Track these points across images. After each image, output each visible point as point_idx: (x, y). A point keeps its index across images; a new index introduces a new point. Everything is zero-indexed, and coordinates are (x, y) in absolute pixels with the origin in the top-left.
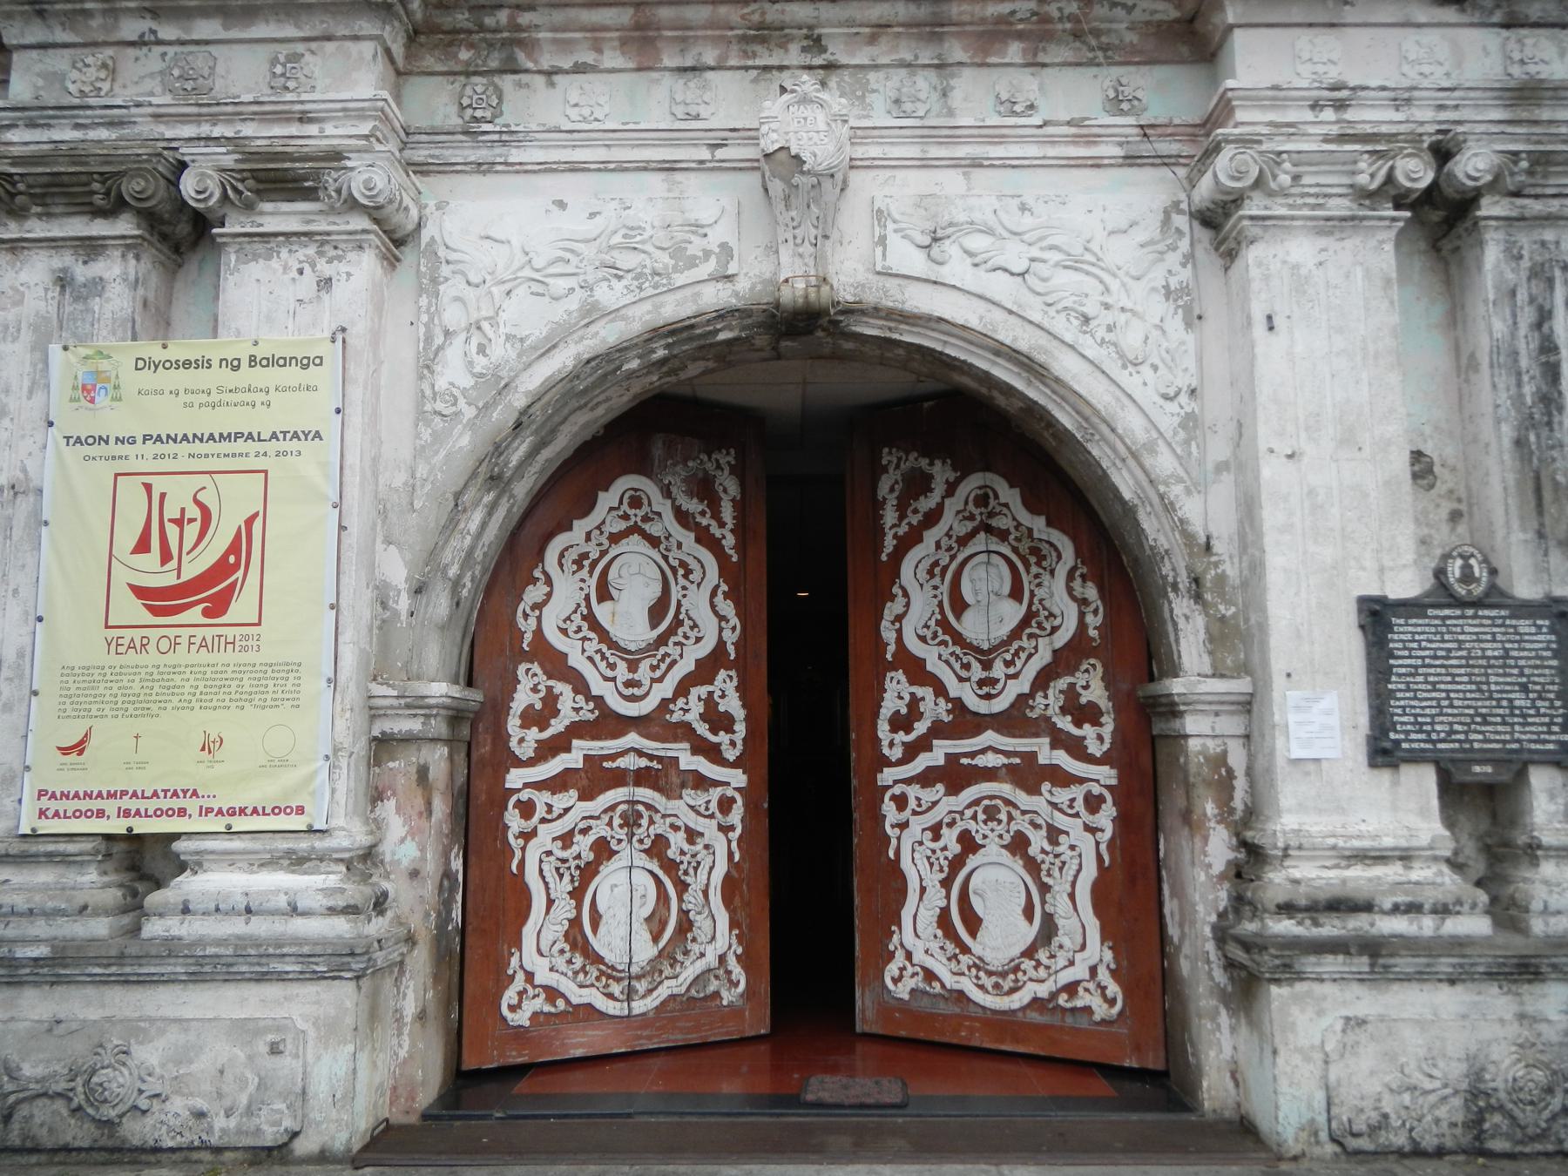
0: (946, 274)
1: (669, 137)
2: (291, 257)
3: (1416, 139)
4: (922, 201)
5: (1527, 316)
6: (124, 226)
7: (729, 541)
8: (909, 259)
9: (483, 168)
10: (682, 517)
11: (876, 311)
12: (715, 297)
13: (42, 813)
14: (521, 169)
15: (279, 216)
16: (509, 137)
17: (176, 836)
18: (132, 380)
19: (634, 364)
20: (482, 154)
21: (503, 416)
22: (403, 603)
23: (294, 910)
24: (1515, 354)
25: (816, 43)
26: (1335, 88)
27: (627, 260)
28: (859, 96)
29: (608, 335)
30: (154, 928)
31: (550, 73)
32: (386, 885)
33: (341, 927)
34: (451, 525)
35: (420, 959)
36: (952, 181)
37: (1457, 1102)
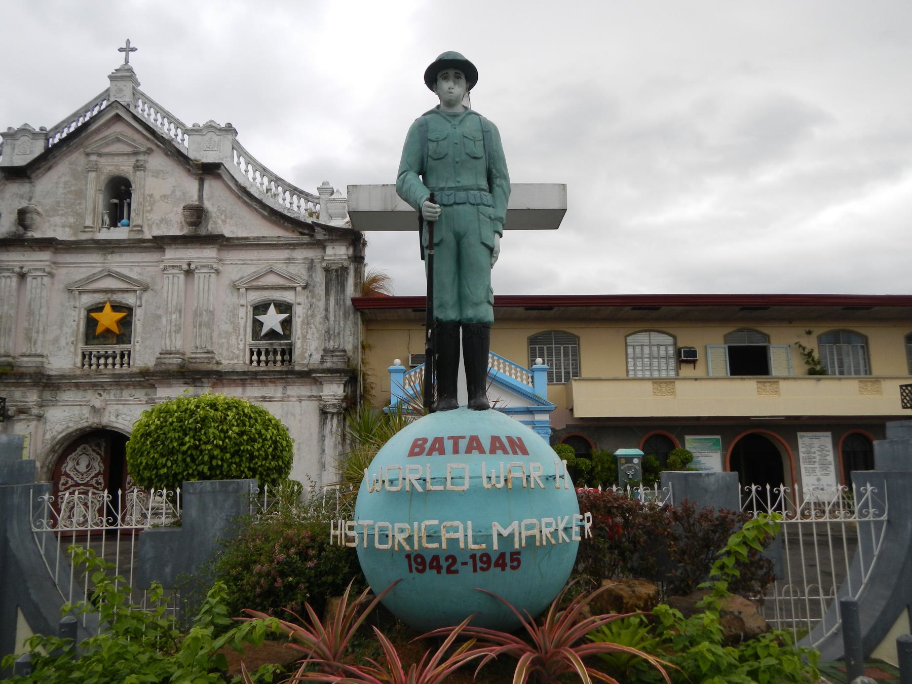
0: (118, 421)
1: (80, 401)
4: (117, 410)
7: (103, 454)
8: (113, 418)
9: (53, 405)
10: (94, 450)
11: (109, 426)
12: (86, 424)
14: (58, 406)
15: (22, 416)
16: (57, 401)
21: (54, 442)
25: (103, 387)
27: (73, 419)
28: (109, 393)
29: (70, 430)
34: (46, 458)
36: (121, 407)
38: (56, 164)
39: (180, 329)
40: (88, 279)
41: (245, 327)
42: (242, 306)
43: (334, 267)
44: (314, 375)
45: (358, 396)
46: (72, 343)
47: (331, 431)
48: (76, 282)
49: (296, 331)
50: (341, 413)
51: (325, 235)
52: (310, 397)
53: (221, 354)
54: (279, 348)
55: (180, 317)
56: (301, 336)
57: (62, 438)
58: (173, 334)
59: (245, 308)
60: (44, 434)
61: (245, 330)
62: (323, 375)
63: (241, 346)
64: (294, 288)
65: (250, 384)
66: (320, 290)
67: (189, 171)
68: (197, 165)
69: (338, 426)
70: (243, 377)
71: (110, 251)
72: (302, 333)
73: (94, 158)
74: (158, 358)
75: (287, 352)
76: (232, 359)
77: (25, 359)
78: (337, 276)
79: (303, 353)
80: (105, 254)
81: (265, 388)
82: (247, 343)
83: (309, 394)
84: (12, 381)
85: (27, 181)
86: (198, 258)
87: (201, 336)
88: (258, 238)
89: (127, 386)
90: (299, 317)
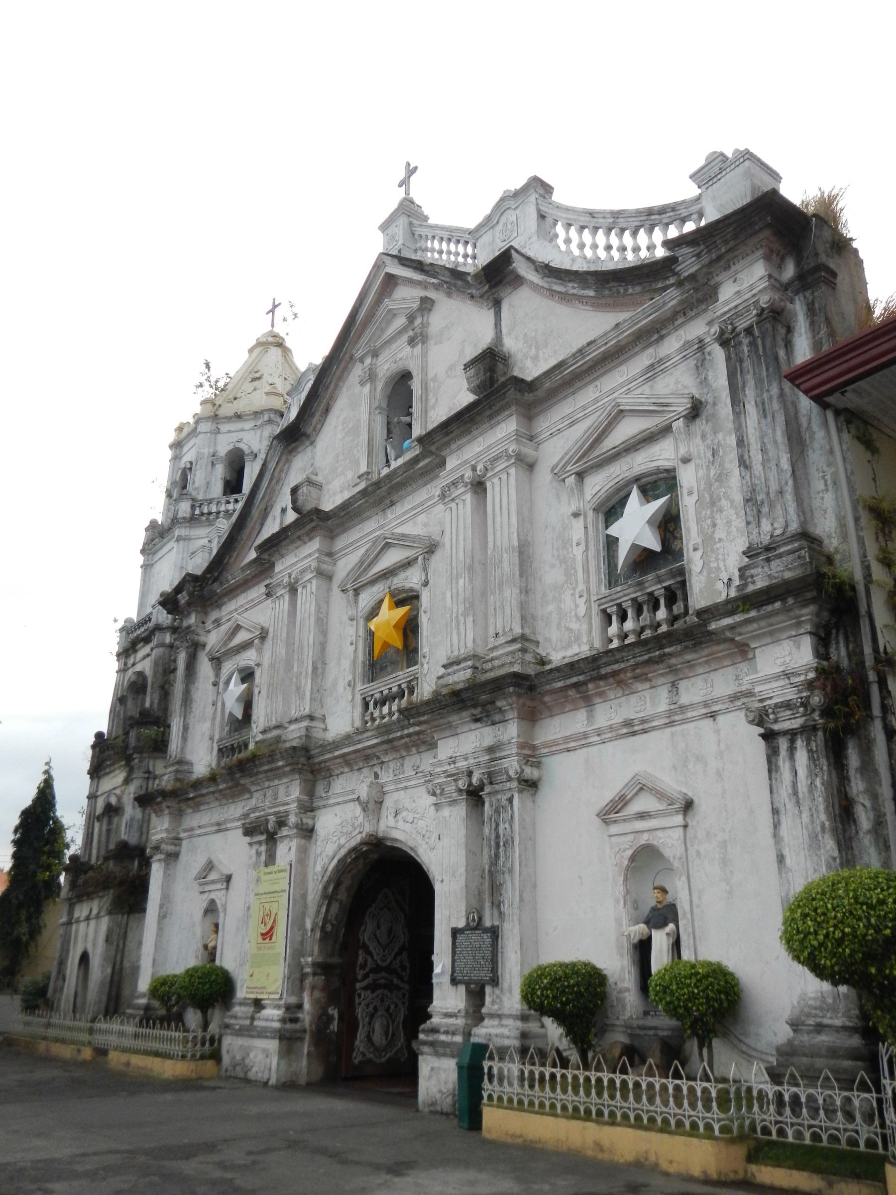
2: (286, 841)
3: (463, 773)
5: (494, 825)
6: (263, 837)
9: (324, 806)
12: (358, 839)
13: (247, 993)
15: (285, 831)
16: (328, 798)
17: (261, 1000)
18: (264, 878)
19: (349, 860)
20: (323, 803)
21: (326, 879)
22: (309, 934)
23: (273, 1020)
24: (490, 840)
25: (378, 758)
26: (451, 758)
29: (343, 852)
30: (256, 1023)
31: (338, 775)
32: (300, 1015)
33: (277, 1025)
34: (318, 912)
35: (307, 1037)
37: (450, 1097)
38: (332, 399)
39: (472, 605)
40: (363, 563)
41: (586, 562)
42: (576, 515)
43: (742, 324)
44: (713, 626)
45: (869, 662)
46: (349, 685)
47: (795, 793)
48: (348, 574)
49: (688, 530)
50: (814, 728)
51: (698, 255)
52: (734, 698)
53: (548, 640)
54: (658, 589)
55: (471, 580)
56: (699, 540)
57: (337, 866)
58: (461, 619)
59: (582, 517)
60: (315, 864)
61: (586, 571)
62: (738, 618)
63: (582, 610)
64: (666, 430)
65: (601, 694)
66: (725, 409)
67: (472, 297)
68: (476, 276)
69: (812, 774)
70: (574, 680)
71: (388, 501)
72: (701, 531)
73: (368, 361)
74: (439, 678)
75: (679, 594)
76: (569, 646)
77: (293, 727)
78: (753, 344)
79: (711, 582)
80: (384, 510)
81: (633, 699)
82: (594, 598)
83: (731, 689)
84: (266, 768)
85: (308, 443)
86: (489, 447)
87: (503, 607)
88: (580, 351)
89: (407, 747)
90: (690, 493)
